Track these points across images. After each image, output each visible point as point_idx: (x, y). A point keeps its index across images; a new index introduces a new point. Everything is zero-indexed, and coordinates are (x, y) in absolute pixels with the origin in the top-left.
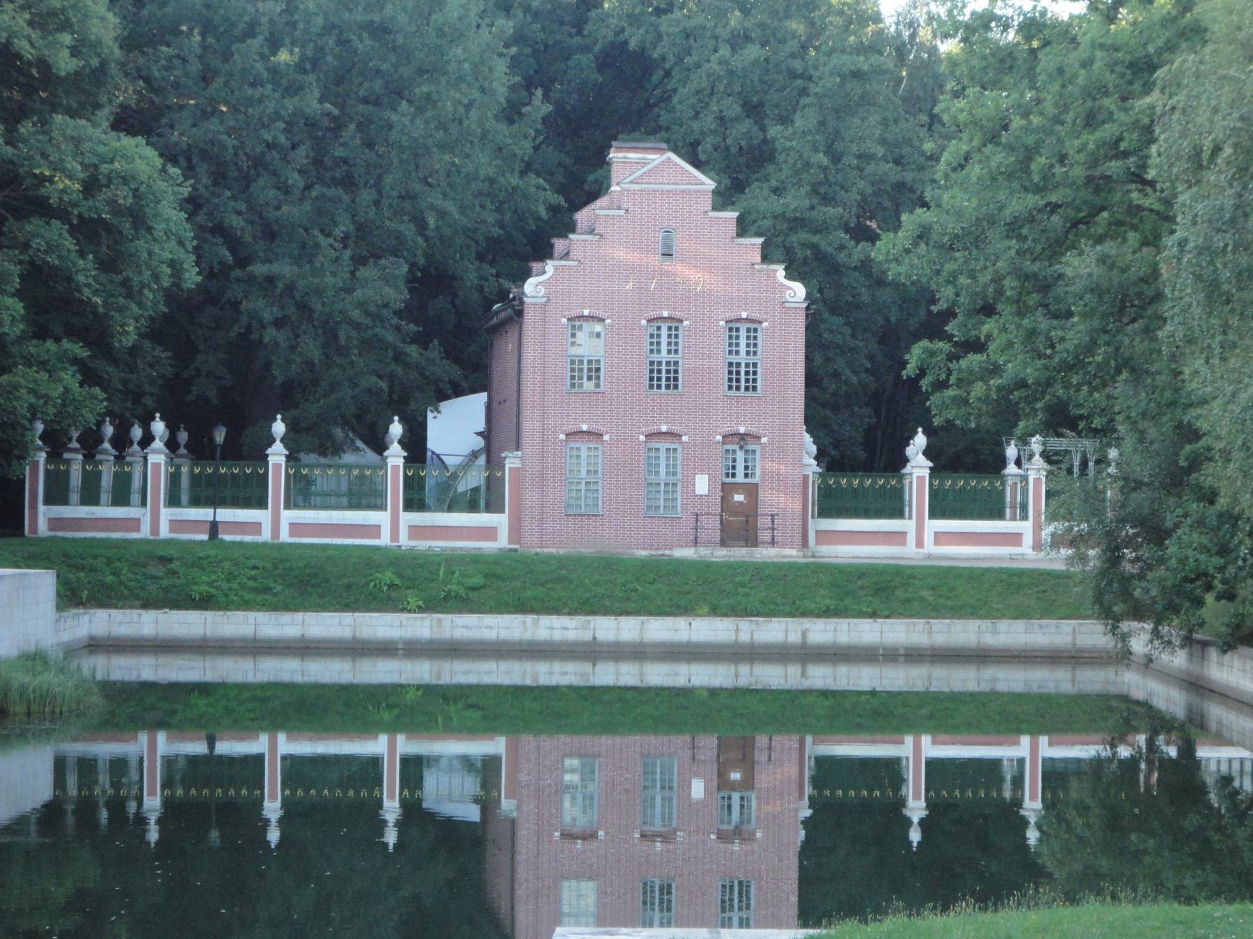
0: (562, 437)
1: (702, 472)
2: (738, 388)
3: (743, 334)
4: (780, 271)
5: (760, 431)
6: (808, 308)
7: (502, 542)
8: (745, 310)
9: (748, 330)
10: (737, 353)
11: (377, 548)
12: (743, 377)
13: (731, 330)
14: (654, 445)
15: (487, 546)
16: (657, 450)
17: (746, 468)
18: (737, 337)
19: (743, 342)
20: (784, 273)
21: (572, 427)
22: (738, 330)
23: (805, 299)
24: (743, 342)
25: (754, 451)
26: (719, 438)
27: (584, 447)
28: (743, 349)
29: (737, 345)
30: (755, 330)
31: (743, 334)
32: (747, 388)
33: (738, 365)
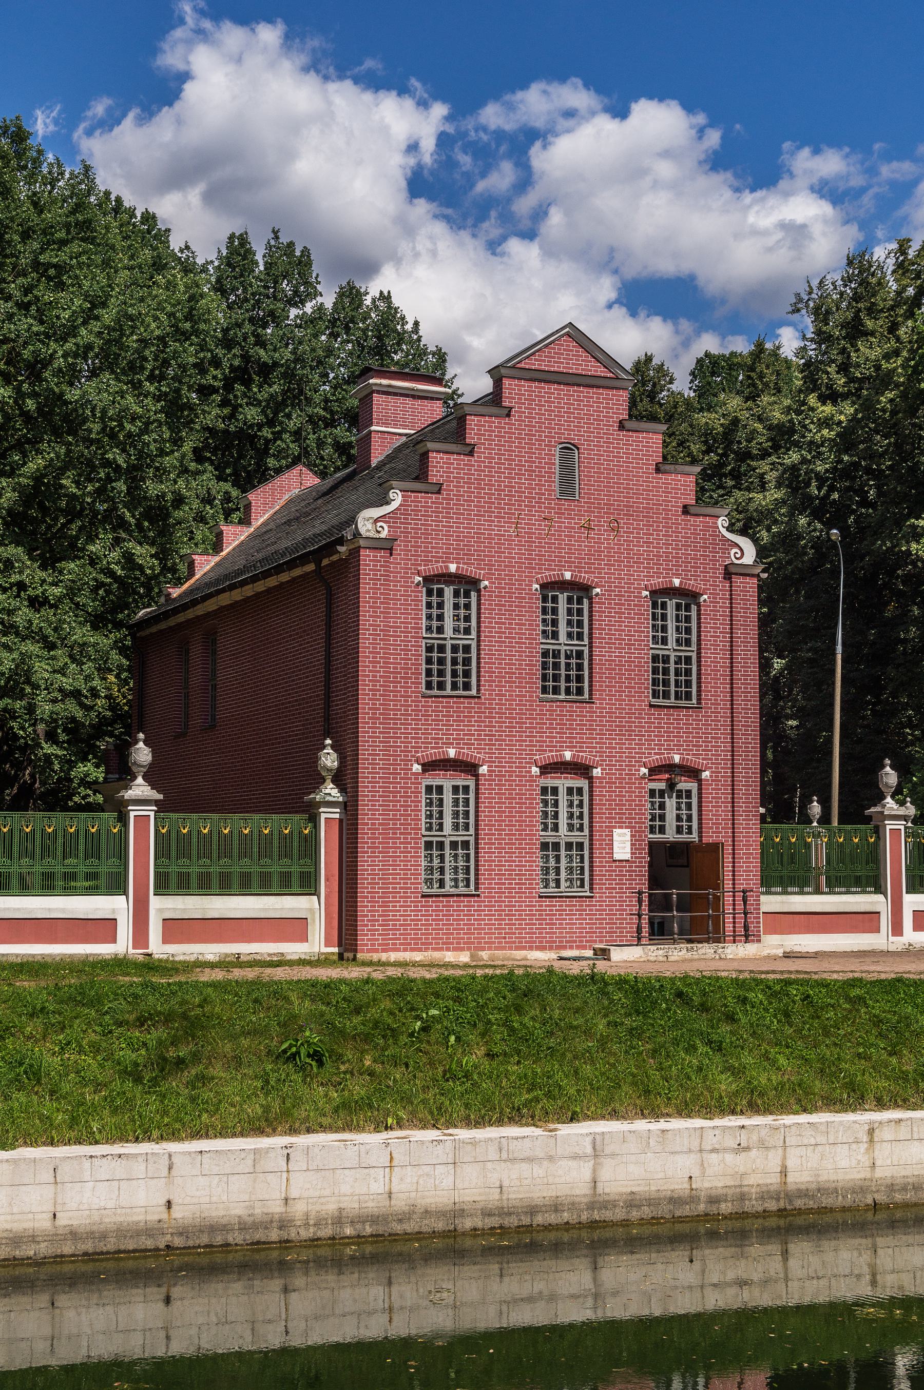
0: (417, 768)
5: (699, 762)
8: (678, 575)
14: (549, 782)
15: (293, 950)
16: (555, 791)
21: (432, 753)
24: (671, 624)
25: (689, 793)
26: (644, 771)
30: (688, 608)
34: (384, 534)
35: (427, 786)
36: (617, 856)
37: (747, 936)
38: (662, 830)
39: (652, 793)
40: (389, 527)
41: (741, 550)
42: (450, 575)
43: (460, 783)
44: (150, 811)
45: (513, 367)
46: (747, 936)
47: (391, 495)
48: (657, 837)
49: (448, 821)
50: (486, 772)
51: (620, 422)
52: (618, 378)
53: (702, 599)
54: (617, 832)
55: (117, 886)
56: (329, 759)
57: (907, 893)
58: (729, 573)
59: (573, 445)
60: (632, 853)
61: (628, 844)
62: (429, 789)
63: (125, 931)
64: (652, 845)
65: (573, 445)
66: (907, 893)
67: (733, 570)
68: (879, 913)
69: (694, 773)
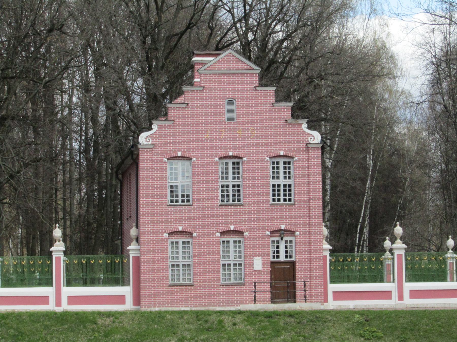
1: (259, 256)
2: (279, 200)
3: (281, 165)
4: (305, 126)
7: (129, 306)
9: (285, 163)
10: (278, 178)
12: (282, 193)
13: (273, 163)
17: (286, 252)
18: (278, 168)
19: (281, 170)
20: (306, 125)
21: (172, 229)
22: (278, 163)
23: (321, 142)
24: (281, 170)
26: (268, 233)
27: (180, 241)
28: (282, 175)
29: (278, 173)
31: (281, 165)
32: (285, 200)
33: (279, 186)
34: (150, 143)
35: (171, 242)
36: (255, 269)
37: (306, 300)
38: (278, 257)
39: (273, 242)
40: (152, 140)
41: (313, 136)
42: (179, 157)
43: (186, 240)
44: (61, 255)
45: (205, 70)
46: (306, 300)
47: (153, 126)
48: (276, 260)
49: (181, 255)
50: (196, 235)
51: (255, 87)
52: (253, 69)
53: (295, 159)
54: (255, 259)
55: (49, 283)
56: (133, 232)
57: (406, 282)
58: (307, 146)
59: (232, 98)
60: (262, 268)
61: (261, 264)
62: (172, 243)
63: (52, 300)
64: (272, 263)
65: (232, 98)
66: (406, 282)
67: (309, 145)
68: (391, 291)
69: (292, 233)
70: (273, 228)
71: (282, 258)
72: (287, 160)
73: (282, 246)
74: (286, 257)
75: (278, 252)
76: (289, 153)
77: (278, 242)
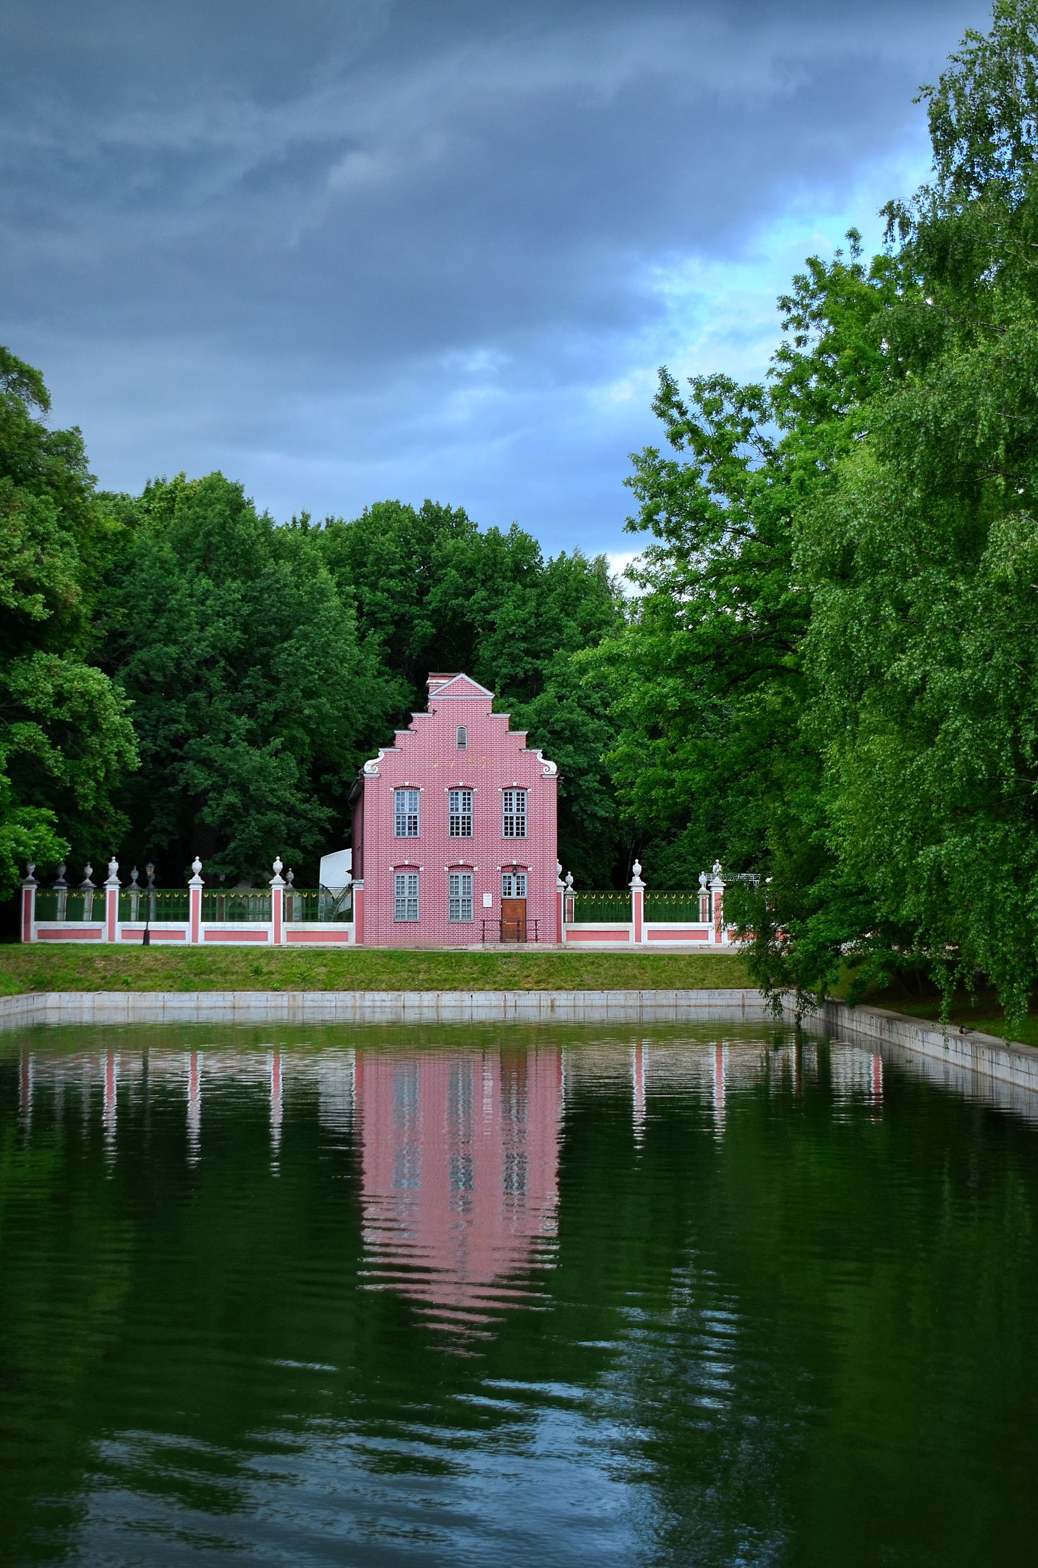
2: (512, 834)
3: (514, 797)
6: (558, 779)
9: (518, 794)
10: (511, 810)
11: (183, 947)
13: (506, 794)
17: (518, 888)
18: (511, 799)
19: (514, 802)
22: (511, 794)
24: (514, 802)
26: (499, 868)
28: (514, 807)
30: (523, 794)
31: (514, 797)
32: (518, 834)
38: (510, 894)
39: (505, 877)
48: (507, 897)
70: (504, 863)
71: (514, 896)
72: (521, 791)
73: (514, 880)
74: (518, 894)
75: (510, 888)
76: (522, 785)
77: (510, 877)
